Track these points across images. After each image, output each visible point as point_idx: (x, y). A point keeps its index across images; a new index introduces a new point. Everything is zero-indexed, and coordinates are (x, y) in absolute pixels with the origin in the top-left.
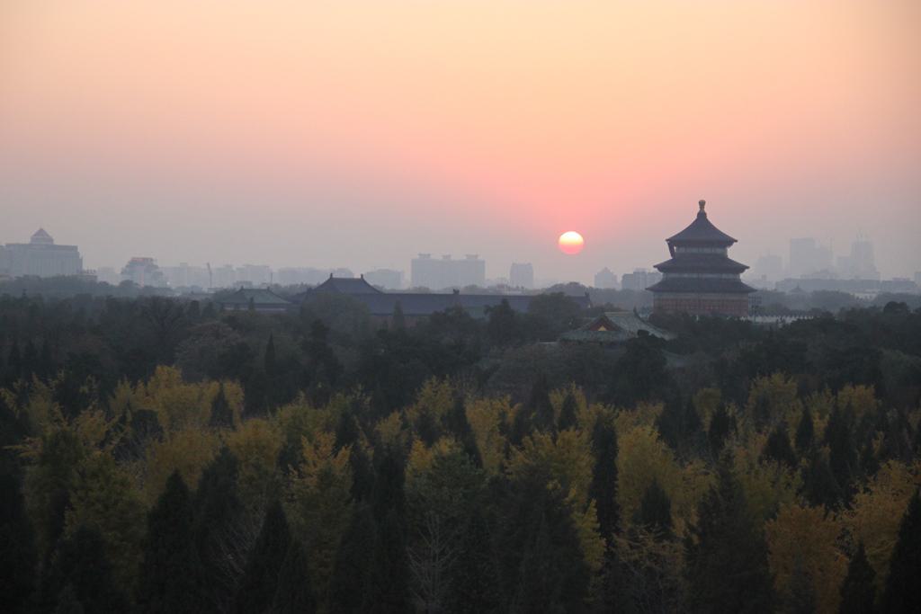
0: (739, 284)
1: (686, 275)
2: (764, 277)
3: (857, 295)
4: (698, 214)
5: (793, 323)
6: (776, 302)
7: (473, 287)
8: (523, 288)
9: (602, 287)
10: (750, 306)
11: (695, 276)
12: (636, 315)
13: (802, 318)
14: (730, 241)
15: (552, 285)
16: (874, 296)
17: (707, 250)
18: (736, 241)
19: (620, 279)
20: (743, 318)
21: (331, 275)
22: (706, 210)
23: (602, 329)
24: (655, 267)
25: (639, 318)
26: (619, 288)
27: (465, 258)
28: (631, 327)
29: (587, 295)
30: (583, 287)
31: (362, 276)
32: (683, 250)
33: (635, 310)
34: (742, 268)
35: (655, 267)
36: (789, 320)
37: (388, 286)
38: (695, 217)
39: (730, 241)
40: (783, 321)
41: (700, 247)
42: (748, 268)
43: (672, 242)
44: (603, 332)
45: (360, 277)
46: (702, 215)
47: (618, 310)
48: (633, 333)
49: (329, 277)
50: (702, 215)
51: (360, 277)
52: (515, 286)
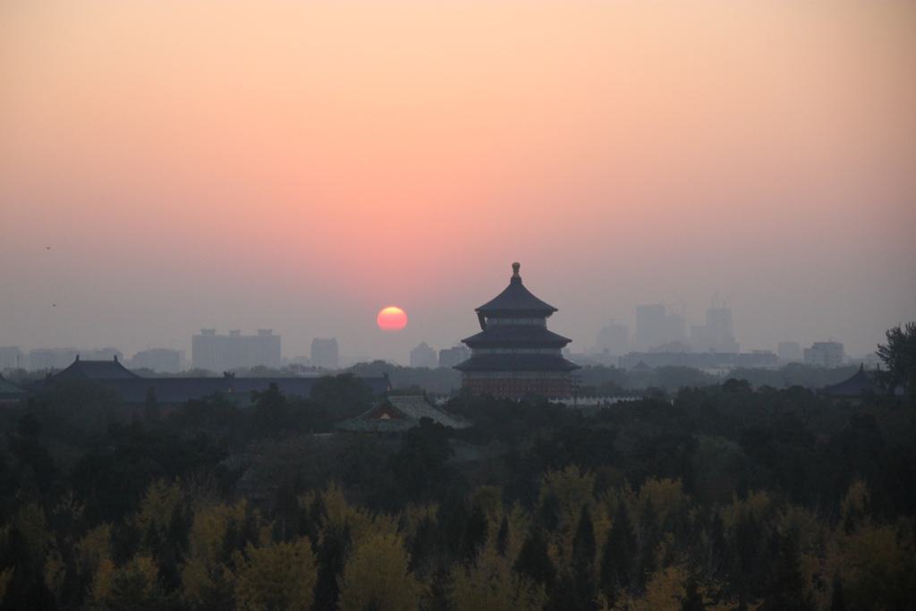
1: (499, 351)
3: (706, 371)
4: (513, 279)
7: (261, 368)
11: (509, 351)
14: (549, 311)
16: (727, 371)
17: (523, 322)
18: (556, 310)
21: (78, 357)
22: (521, 274)
24: (463, 341)
27: (200, 333)
29: (386, 376)
31: (116, 357)
32: (495, 321)
34: (563, 342)
37: (161, 368)
38: (509, 283)
39: (549, 311)
41: (515, 317)
43: (482, 312)
44: (384, 420)
45: (113, 359)
46: (516, 280)
49: (74, 360)
50: (516, 280)
51: (113, 359)
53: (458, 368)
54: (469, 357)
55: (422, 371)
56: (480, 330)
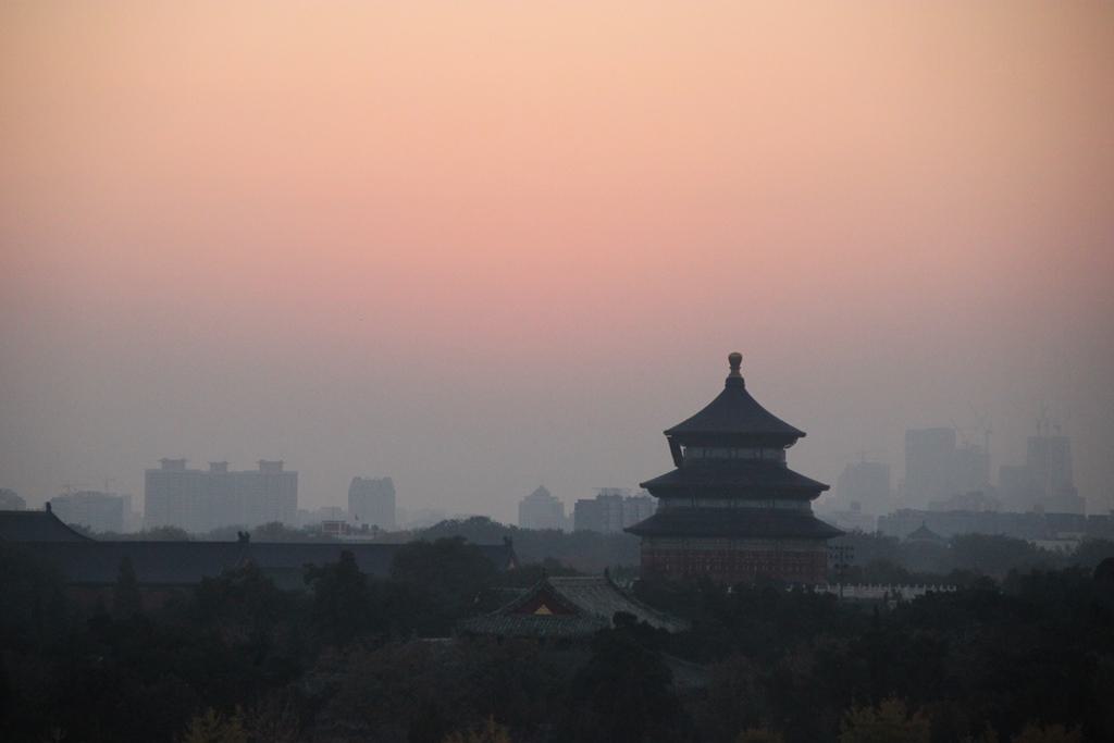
1: (704, 503)
2: (856, 506)
3: (1040, 544)
4: (728, 380)
5: (919, 600)
6: (876, 555)
7: (275, 527)
8: (375, 528)
9: (532, 525)
10: (831, 565)
11: (723, 504)
12: (610, 583)
13: (933, 589)
14: (791, 435)
15: (438, 521)
17: (746, 454)
18: (803, 435)
19: (569, 510)
20: (816, 590)
22: (745, 370)
23: (543, 610)
24: (642, 485)
25: (616, 588)
26: (569, 528)
28: (602, 607)
29: (509, 543)
30: (497, 527)
32: (698, 453)
33: (607, 572)
34: (816, 489)
35: (642, 485)
36: (909, 594)
37: (98, 527)
38: (721, 387)
39: (791, 435)
40: (897, 596)
41: (732, 444)
42: (826, 488)
43: (676, 436)
44: (543, 617)
46: (735, 383)
47: (572, 572)
48: (603, 619)
50: (735, 383)
52: (359, 526)
54: (654, 513)
55: (553, 536)
56: (668, 465)
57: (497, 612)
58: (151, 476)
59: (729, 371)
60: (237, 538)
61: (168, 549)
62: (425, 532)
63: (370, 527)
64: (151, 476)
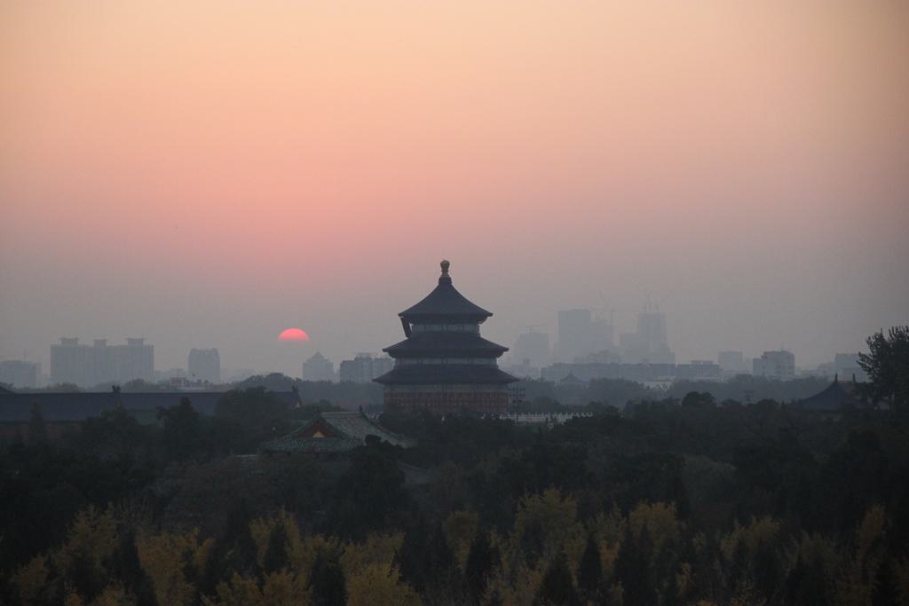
0: (494, 370)
1: (426, 362)
5: (568, 423)
6: (542, 395)
7: (138, 382)
8: (207, 381)
9: (314, 379)
10: (510, 401)
11: (437, 361)
12: (364, 416)
13: (578, 415)
14: (483, 315)
15: (248, 376)
17: (453, 328)
18: (491, 315)
19: (336, 367)
22: (451, 273)
23: (318, 435)
24: (384, 350)
26: (336, 380)
29: (295, 390)
30: (288, 380)
32: (421, 328)
33: (361, 408)
34: (499, 351)
35: (384, 350)
39: (483, 315)
40: (554, 420)
41: (444, 324)
42: (507, 350)
43: (406, 317)
46: (445, 281)
47: (338, 409)
48: (359, 440)
50: (445, 281)
52: (196, 381)
53: (379, 380)
55: (324, 386)
57: (288, 436)
58: (55, 350)
59: (441, 273)
60: (111, 390)
61: (66, 398)
62: (242, 383)
63: (203, 381)
64: (55, 350)
